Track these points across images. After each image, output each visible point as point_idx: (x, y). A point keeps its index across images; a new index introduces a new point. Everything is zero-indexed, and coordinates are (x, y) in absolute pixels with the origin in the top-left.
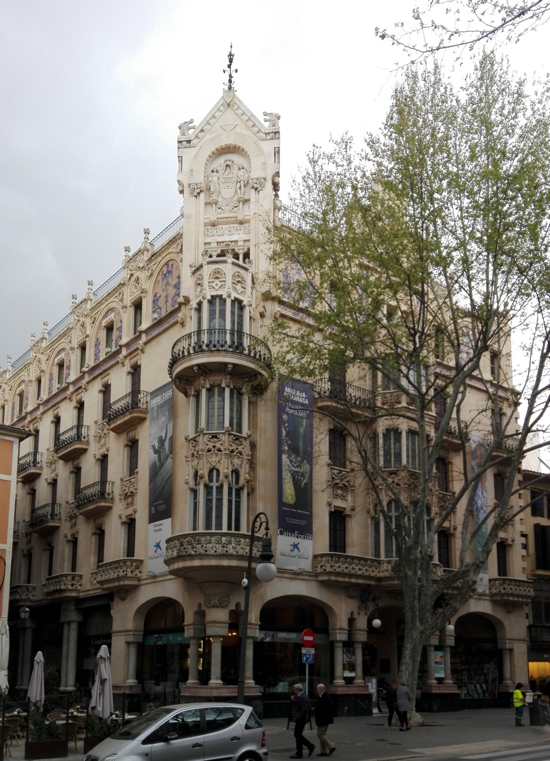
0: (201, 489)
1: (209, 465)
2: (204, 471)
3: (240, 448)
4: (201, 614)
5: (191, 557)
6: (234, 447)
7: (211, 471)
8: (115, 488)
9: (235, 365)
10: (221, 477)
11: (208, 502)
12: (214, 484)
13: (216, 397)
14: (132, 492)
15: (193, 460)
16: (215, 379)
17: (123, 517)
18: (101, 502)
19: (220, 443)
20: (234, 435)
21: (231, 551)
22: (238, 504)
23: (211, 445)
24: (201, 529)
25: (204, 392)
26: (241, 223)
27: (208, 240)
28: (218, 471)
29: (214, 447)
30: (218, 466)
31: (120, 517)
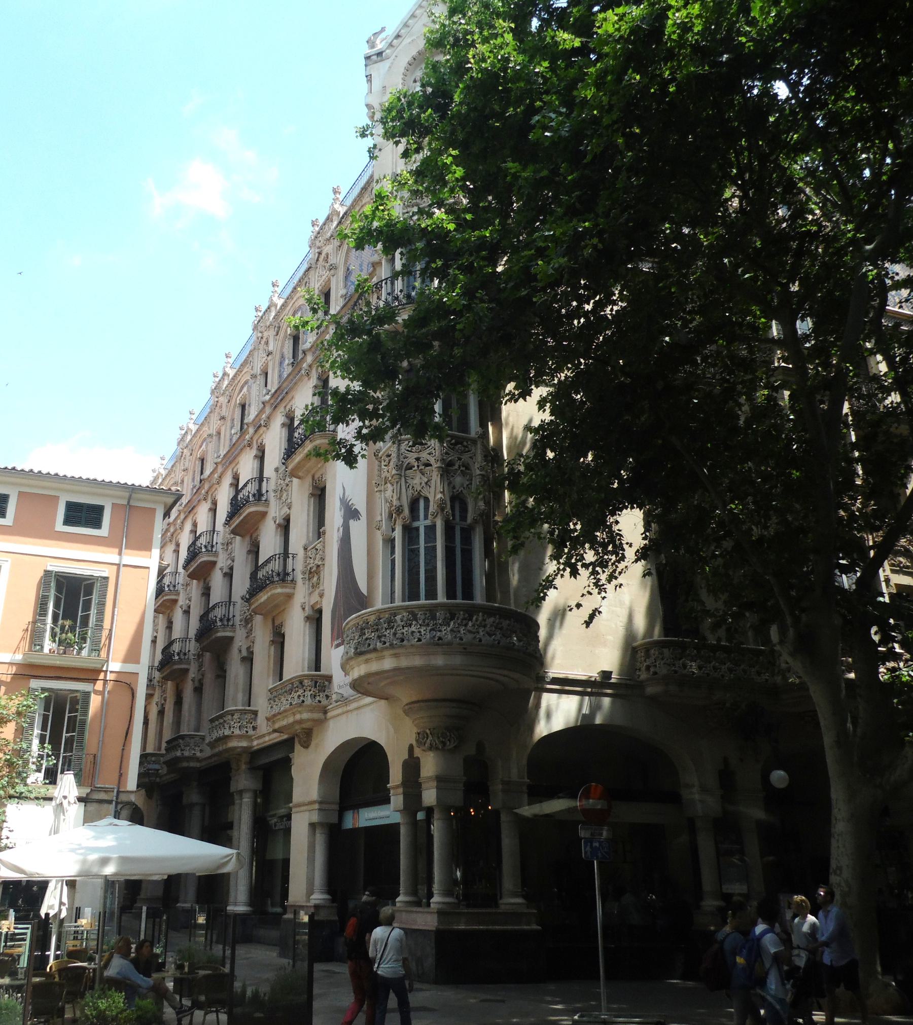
0: (398, 534)
1: (410, 491)
3: (465, 457)
8: (298, 565)
10: (432, 508)
14: (318, 566)
15: (385, 490)
17: (307, 609)
18: (276, 588)
19: (428, 451)
20: (453, 437)
22: (467, 555)
24: (398, 603)
28: (427, 500)
29: (418, 459)
30: (425, 493)
31: (304, 609)
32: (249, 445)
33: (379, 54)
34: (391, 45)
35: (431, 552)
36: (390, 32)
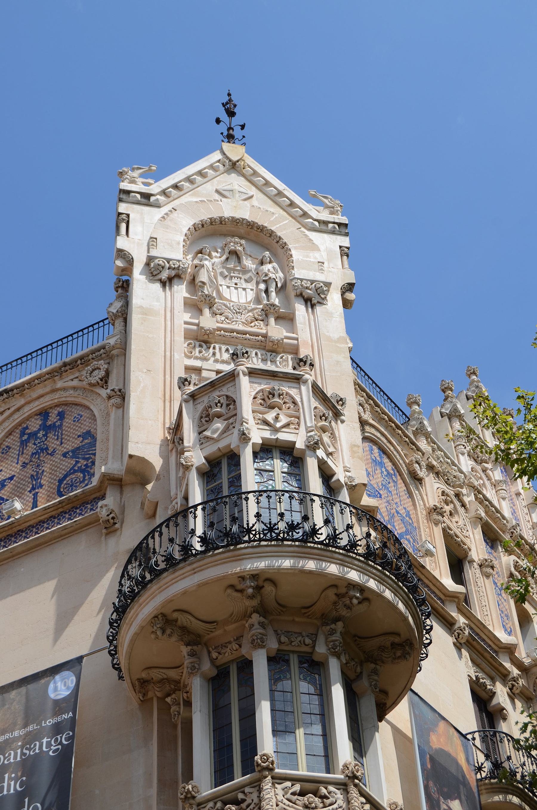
33: (146, 196)
34: (164, 193)
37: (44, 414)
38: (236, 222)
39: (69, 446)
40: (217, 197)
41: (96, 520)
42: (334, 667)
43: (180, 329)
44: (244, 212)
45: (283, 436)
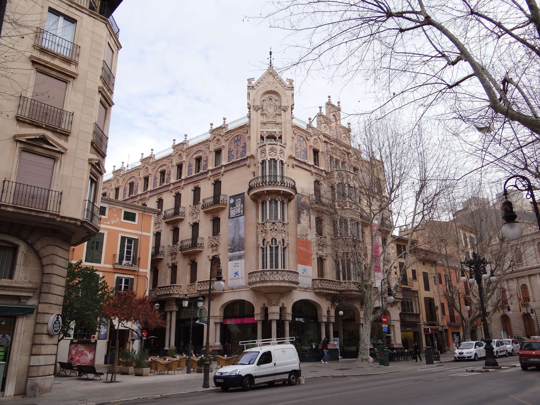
2: (269, 239)
4: (265, 311)
5: (266, 281)
6: (282, 229)
7: (272, 239)
9: (283, 191)
10: (277, 243)
11: (271, 254)
12: (274, 246)
13: (273, 205)
16: (274, 196)
21: (286, 279)
23: (272, 228)
25: (268, 202)
26: (277, 124)
27: (262, 130)
28: (275, 240)
30: (276, 238)
32: (171, 192)
33: (253, 87)
35: (277, 254)
36: (256, 79)
37: (237, 136)
38: (271, 91)
39: (242, 146)
40: (267, 84)
41: (246, 165)
42: (279, 202)
43: (259, 122)
44: (273, 89)
45: (274, 158)
